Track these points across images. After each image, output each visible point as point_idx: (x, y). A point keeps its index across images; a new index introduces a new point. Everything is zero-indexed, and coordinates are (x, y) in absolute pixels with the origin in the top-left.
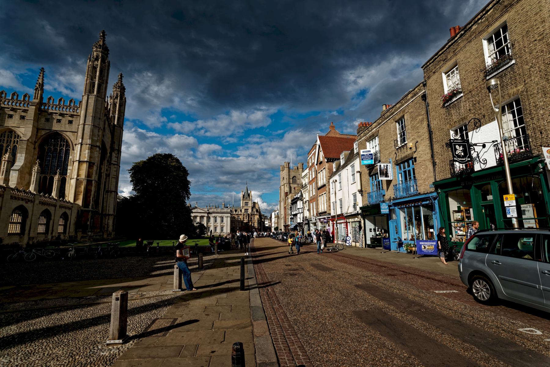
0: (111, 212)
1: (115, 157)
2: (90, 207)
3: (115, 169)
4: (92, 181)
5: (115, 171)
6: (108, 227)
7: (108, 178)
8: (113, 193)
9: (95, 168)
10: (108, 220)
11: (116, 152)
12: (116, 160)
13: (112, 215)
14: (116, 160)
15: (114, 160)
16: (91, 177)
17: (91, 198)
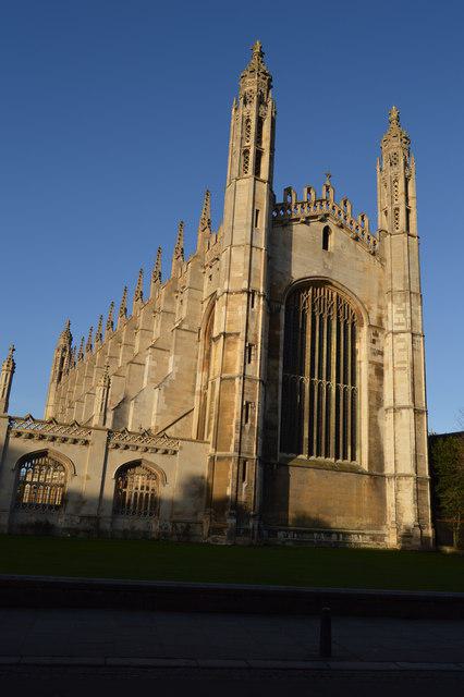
0: (407, 467)
1: (398, 312)
2: (232, 447)
3: (401, 345)
4: (233, 379)
5: (400, 350)
6: (398, 514)
7: (386, 373)
8: (404, 411)
9: (240, 346)
10: (397, 491)
11: (398, 299)
12: (403, 320)
13: (407, 476)
14: (403, 320)
15: (396, 321)
16: (232, 370)
17: (234, 425)
